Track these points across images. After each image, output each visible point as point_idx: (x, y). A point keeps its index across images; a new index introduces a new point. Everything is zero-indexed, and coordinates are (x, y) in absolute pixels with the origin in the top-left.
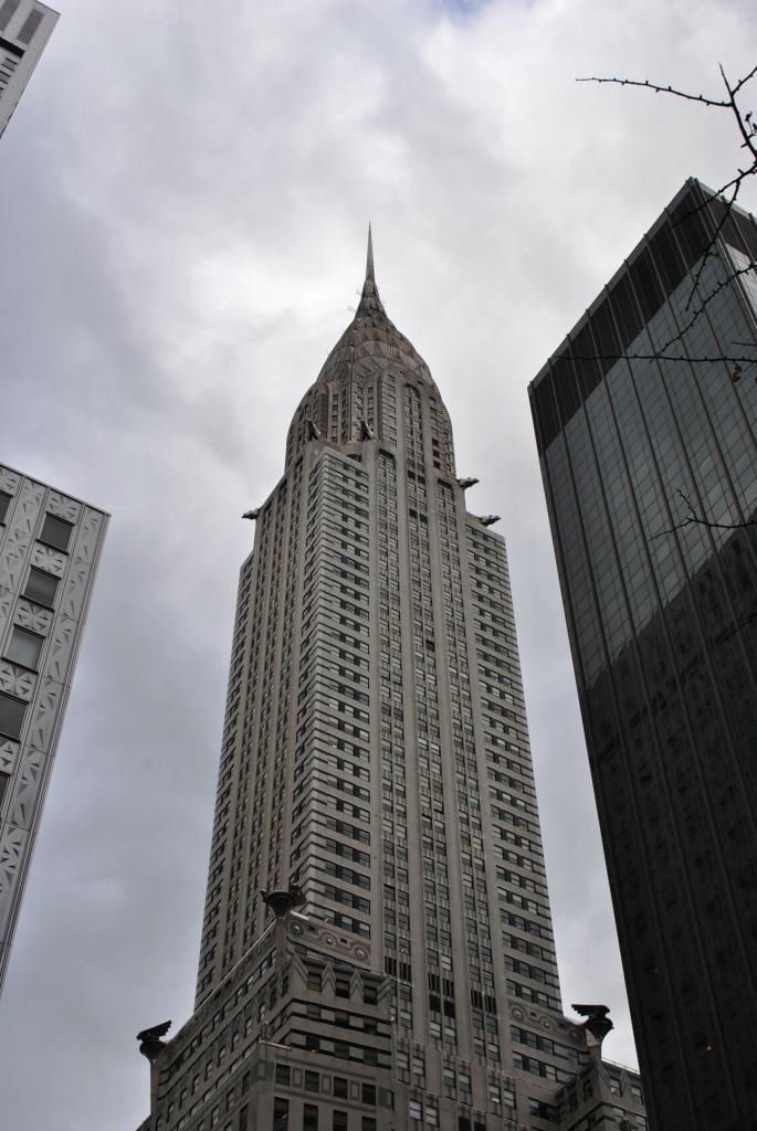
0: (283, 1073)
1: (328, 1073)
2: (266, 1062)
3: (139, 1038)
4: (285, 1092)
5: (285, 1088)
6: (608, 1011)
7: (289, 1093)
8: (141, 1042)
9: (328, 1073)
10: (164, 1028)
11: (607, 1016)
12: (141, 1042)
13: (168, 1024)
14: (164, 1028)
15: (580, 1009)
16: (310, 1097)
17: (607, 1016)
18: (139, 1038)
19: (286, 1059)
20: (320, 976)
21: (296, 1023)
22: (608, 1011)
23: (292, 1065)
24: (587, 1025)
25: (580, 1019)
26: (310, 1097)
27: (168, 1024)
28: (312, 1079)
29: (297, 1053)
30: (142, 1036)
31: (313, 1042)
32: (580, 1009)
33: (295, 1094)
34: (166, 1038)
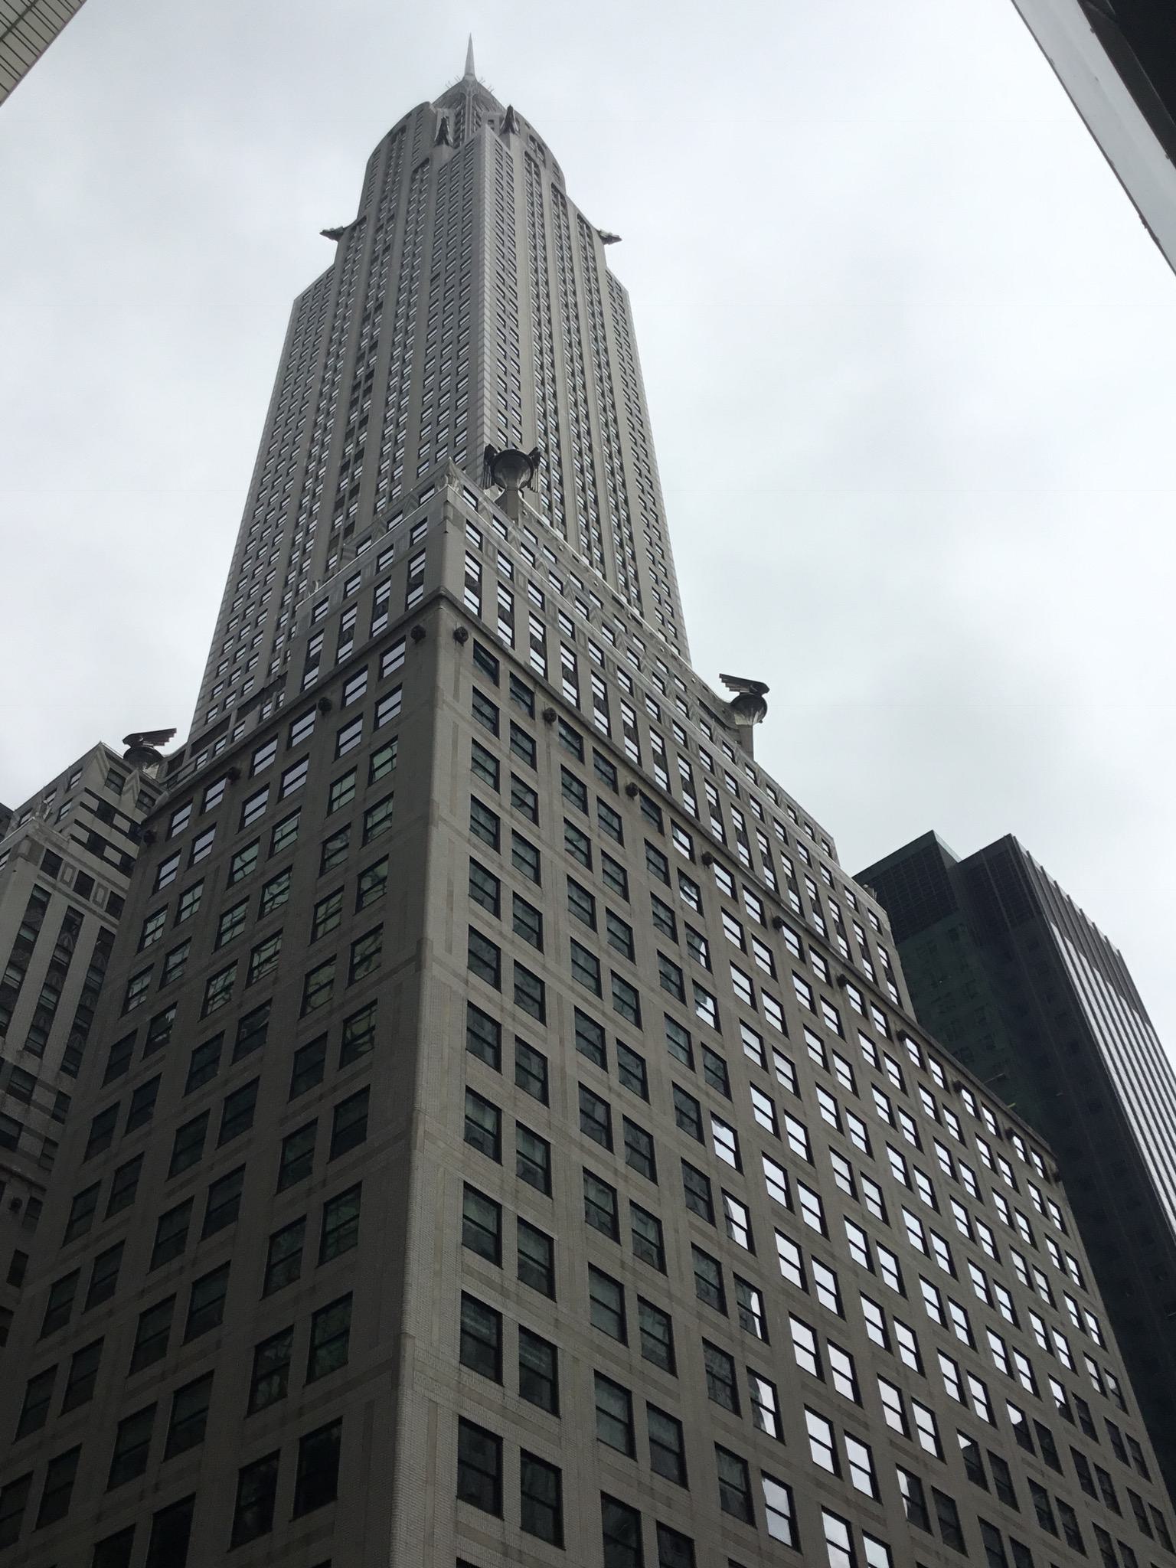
0: (52, 864)
1: (105, 883)
2: (32, 841)
4: (48, 883)
5: (50, 879)
7: (54, 887)
9: (105, 883)
16: (77, 902)
19: (60, 848)
20: (124, 779)
21: (86, 817)
23: (66, 858)
26: (77, 902)
28: (84, 885)
29: (75, 848)
31: (96, 844)
33: (60, 890)
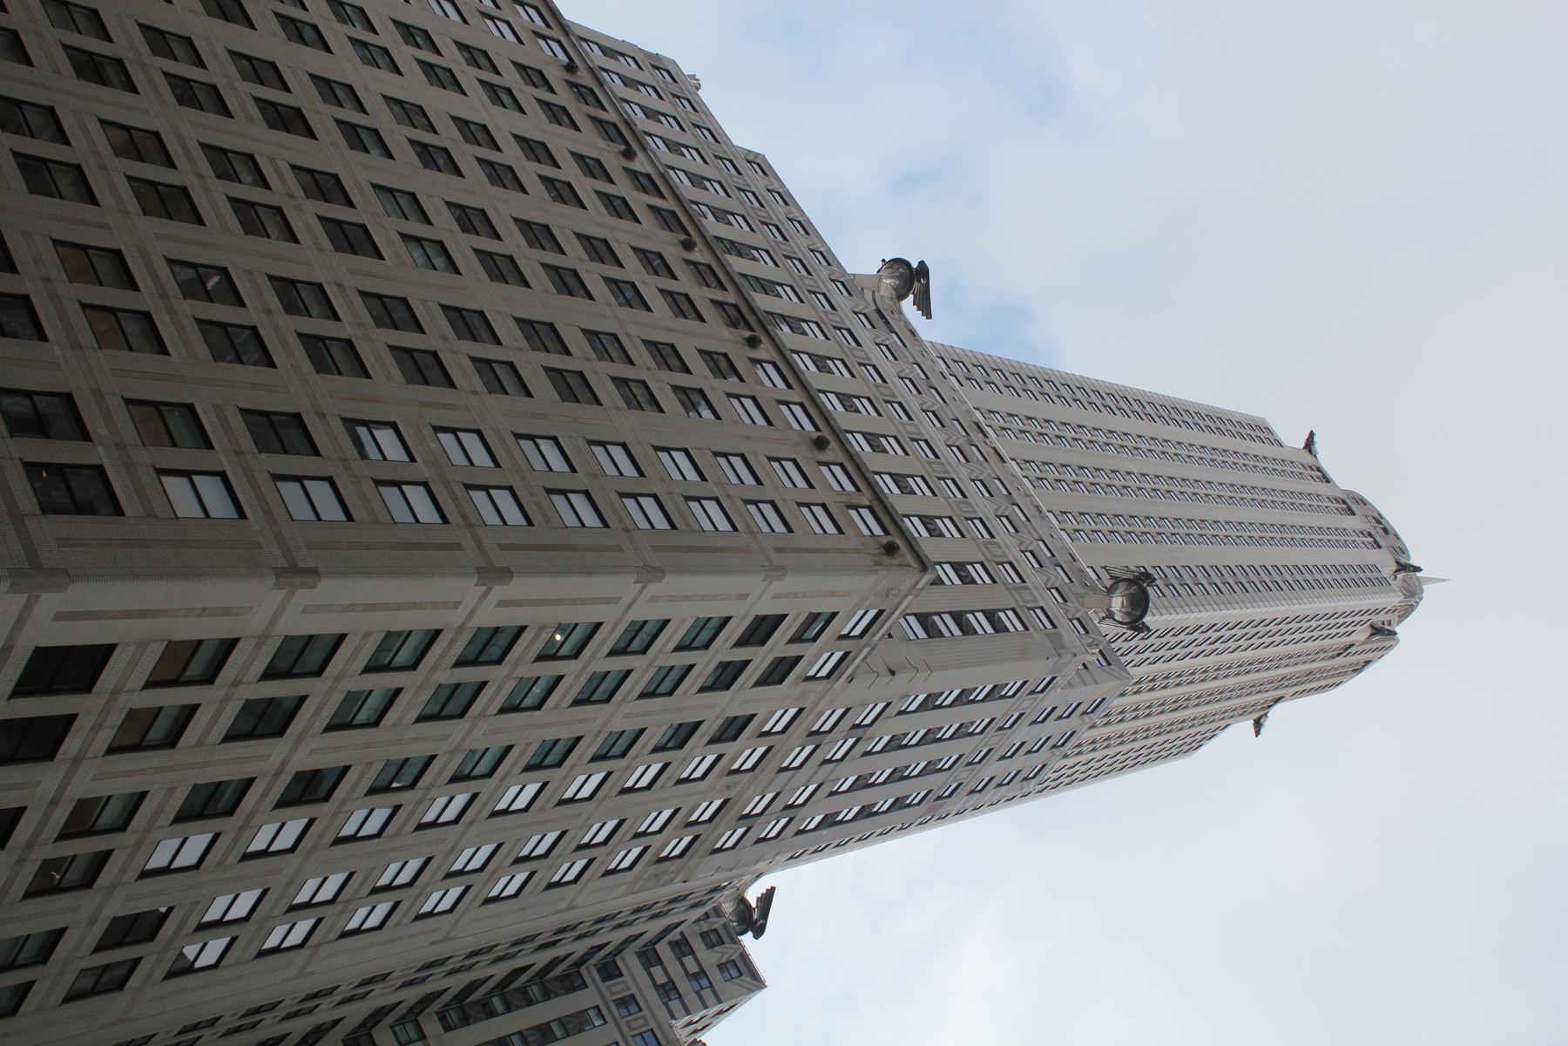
3: (922, 263)
6: (757, 936)
8: (915, 265)
10: (924, 306)
11: (750, 934)
12: (915, 265)
13: (927, 313)
14: (924, 306)
15: (767, 898)
17: (750, 934)
18: (922, 263)
22: (757, 936)
24: (743, 901)
25: (753, 895)
27: (927, 313)
30: (923, 271)
32: (767, 898)
34: (908, 305)
